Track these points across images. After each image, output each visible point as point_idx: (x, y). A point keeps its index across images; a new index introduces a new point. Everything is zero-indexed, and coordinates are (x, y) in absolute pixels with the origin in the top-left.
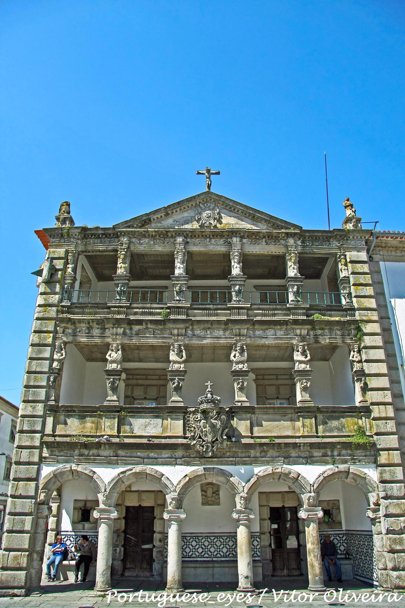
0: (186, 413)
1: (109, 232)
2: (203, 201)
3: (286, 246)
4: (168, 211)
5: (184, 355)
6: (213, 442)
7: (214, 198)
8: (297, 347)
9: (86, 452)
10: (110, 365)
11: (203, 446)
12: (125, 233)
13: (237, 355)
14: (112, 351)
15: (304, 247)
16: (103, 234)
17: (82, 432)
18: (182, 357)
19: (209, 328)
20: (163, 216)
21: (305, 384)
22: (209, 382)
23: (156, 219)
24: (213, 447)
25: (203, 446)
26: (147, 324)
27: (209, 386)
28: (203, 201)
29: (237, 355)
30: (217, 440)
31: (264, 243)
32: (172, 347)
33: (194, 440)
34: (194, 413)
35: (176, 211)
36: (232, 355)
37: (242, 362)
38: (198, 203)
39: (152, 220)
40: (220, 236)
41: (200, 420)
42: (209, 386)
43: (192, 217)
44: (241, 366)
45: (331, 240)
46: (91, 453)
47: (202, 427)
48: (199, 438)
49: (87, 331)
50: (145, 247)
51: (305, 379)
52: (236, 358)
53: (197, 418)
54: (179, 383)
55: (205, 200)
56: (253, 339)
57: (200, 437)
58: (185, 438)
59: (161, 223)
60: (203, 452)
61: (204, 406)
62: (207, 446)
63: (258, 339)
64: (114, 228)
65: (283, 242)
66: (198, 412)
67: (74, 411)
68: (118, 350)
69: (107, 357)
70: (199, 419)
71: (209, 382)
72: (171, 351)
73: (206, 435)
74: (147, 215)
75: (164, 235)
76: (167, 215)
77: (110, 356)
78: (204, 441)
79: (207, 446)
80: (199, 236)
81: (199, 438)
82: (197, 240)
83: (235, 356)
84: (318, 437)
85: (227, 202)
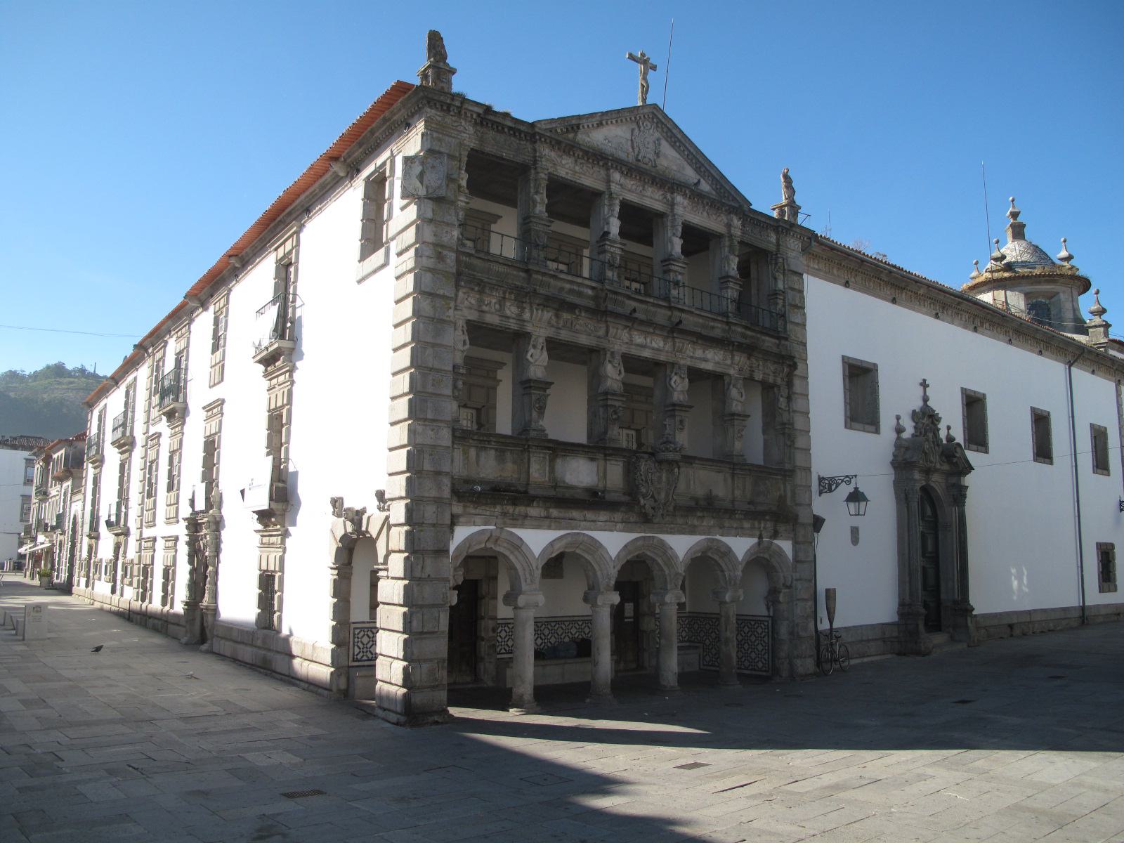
1: (522, 128)
2: (644, 117)
3: (729, 226)
4: (602, 119)
7: (658, 118)
9: (510, 509)
12: (545, 140)
15: (743, 233)
16: (510, 128)
17: (500, 476)
19: (649, 333)
20: (595, 125)
23: (586, 127)
26: (580, 312)
28: (644, 117)
31: (705, 214)
35: (612, 122)
38: (638, 118)
39: (581, 127)
40: (661, 186)
43: (628, 140)
45: (769, 231)
46: (517, 511)
49: (497, 306)
50: (567, 173)
55: (646, 116)
56: (693, 360)
57: (652, 496)
59: (589, 136)
63: (698, 361)
64: (532, 125)
65: (724, 218)
67: (489, 442)
73: (659, 493)
74: (579, 117)
75: (593, 161)
76: (600, 125)
80: (636, 176)
82: (632, 183)
85: (674, 131)
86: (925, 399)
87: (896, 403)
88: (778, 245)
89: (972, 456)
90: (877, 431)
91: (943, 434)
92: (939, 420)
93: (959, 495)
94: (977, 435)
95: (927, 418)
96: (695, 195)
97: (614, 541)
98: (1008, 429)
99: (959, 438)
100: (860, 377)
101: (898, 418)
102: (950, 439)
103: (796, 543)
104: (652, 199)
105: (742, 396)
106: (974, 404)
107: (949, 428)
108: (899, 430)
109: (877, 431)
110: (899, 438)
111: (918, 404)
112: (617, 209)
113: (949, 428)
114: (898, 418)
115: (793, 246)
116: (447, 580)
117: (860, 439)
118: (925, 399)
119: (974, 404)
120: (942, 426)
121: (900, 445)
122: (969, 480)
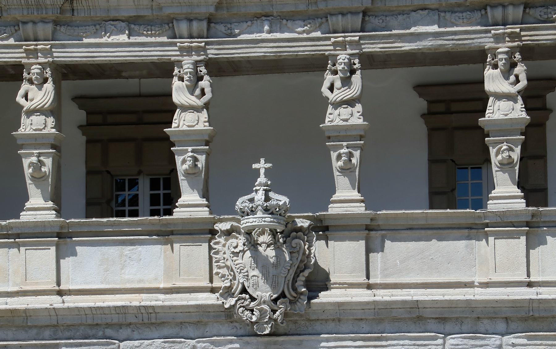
0: (213, 233)
5: (208, 90)
6: (275, 301)
8: (495, 56)
10: (28, 121)
11: (252, 311)
13: (338, 84)
14: (31, 82)
18: (203, 93)
21: (506, 154)
22: (262, 161)
24: (274, 311)
25: (252, 311)
27: (262, 171)
29: (338, 84)
30: (283, 295)
32: (176, 71)
33: (232, 296)
34: (228, 233)
36: (326, 84)
37: (350, 103)
41: (244, 251)
42: (262, 171)
44: (345, 112)
47: (248, 267)
48: (241, 293)
51: (507, 141)
52: (336, 91)
53: (236, 247)
54: (195, 160)
57: (244, 291)
58: (213, 290)
60: (253, 323)
61: (248, 222)
62: (261, 310)
66: (239, 233)
68: (45, 80)
69: (20, 99)
70: (240, 248)
71: (262, 161)
72: (175, 79)
77: (26, 96)
78: (253, 299)
79: (261, 310)
81: (241, 293)
83: (331, 88)
84: (530, 285)
105: (517, 81)
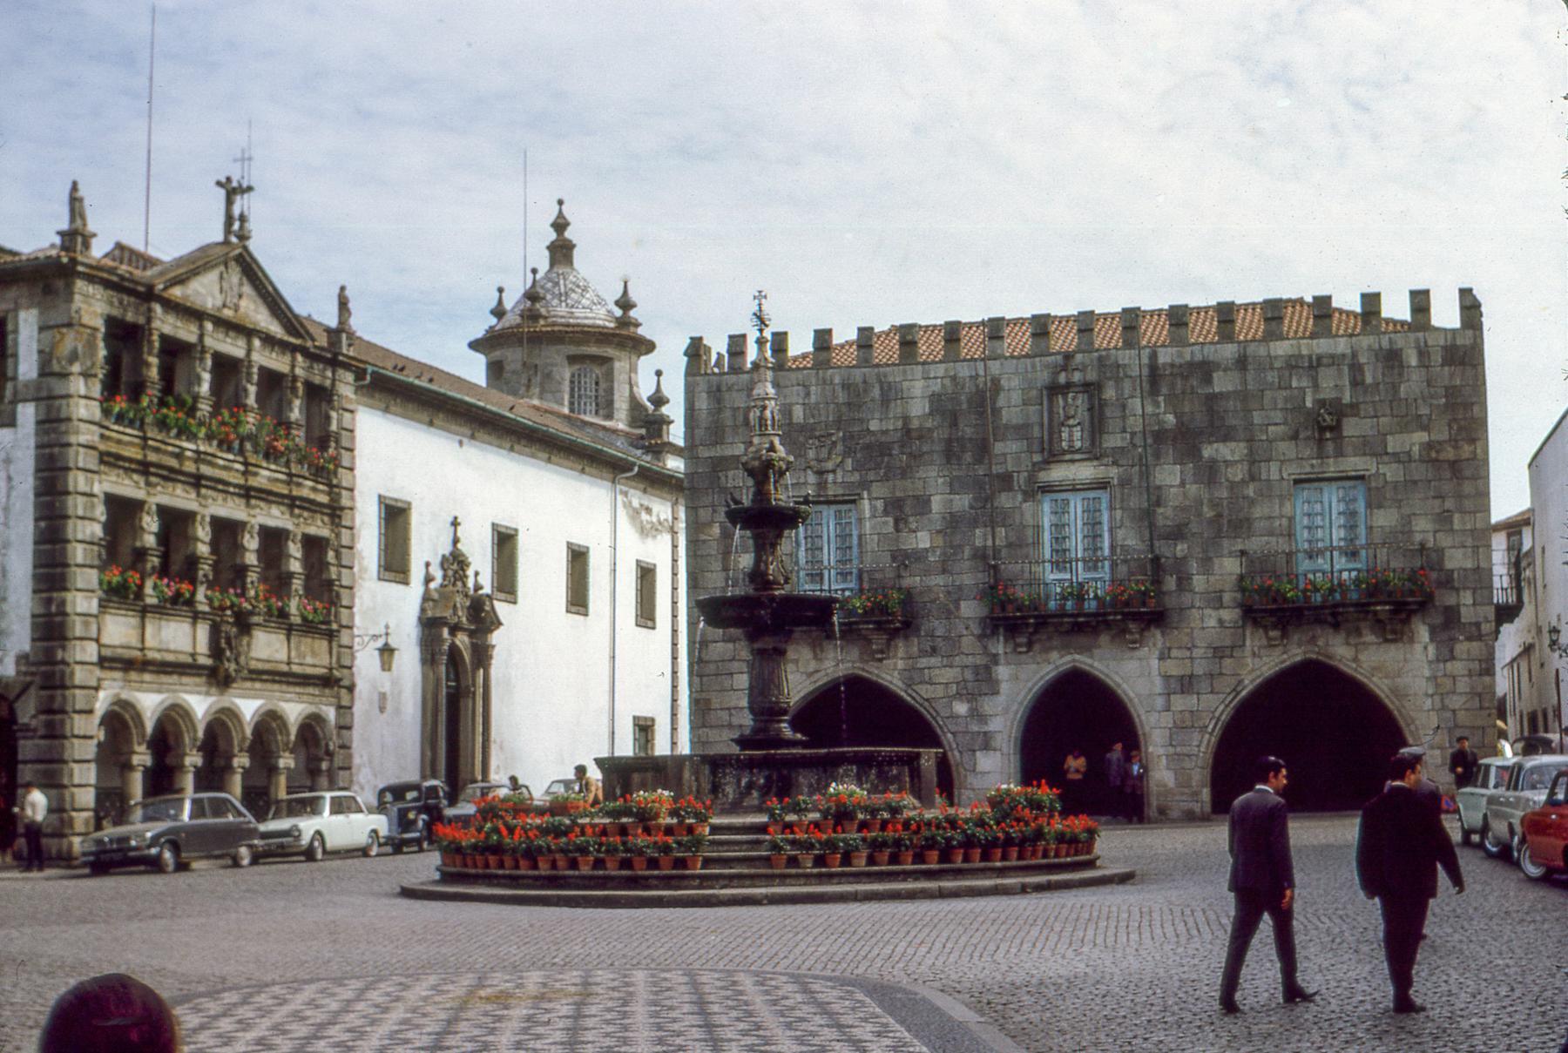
86: (456, 541)
87: (426, 548)
88: (334, 380)
89: (501, 608)
90: (406, 583)
91: (471, 583)
92: (468, 565)
93: (482, 655)
94: (506, 581)
95: (456, 563)
96: (269, 341)
97: (200, 704)
98: (541, 574)
99: (487, 590)
100: (395, 516)
101: (428, 565)
102: (478, 587)
103: (339, 707)
104: (234, 347)
106: (505, 541)
107: (477, 574)
108: (428, 579)
109: (406, 583)
110: (427, 590)
111: (446, 549)
112: (209, 363)
113: (477, 574)
114: (428, 565)
115: (346, 387)
116: (91, 737)
117: (395, 589)
118: (456, 541)
119: (505, 541)
120: (470, 572)
121: (426, 598)
122: (496, 638)
